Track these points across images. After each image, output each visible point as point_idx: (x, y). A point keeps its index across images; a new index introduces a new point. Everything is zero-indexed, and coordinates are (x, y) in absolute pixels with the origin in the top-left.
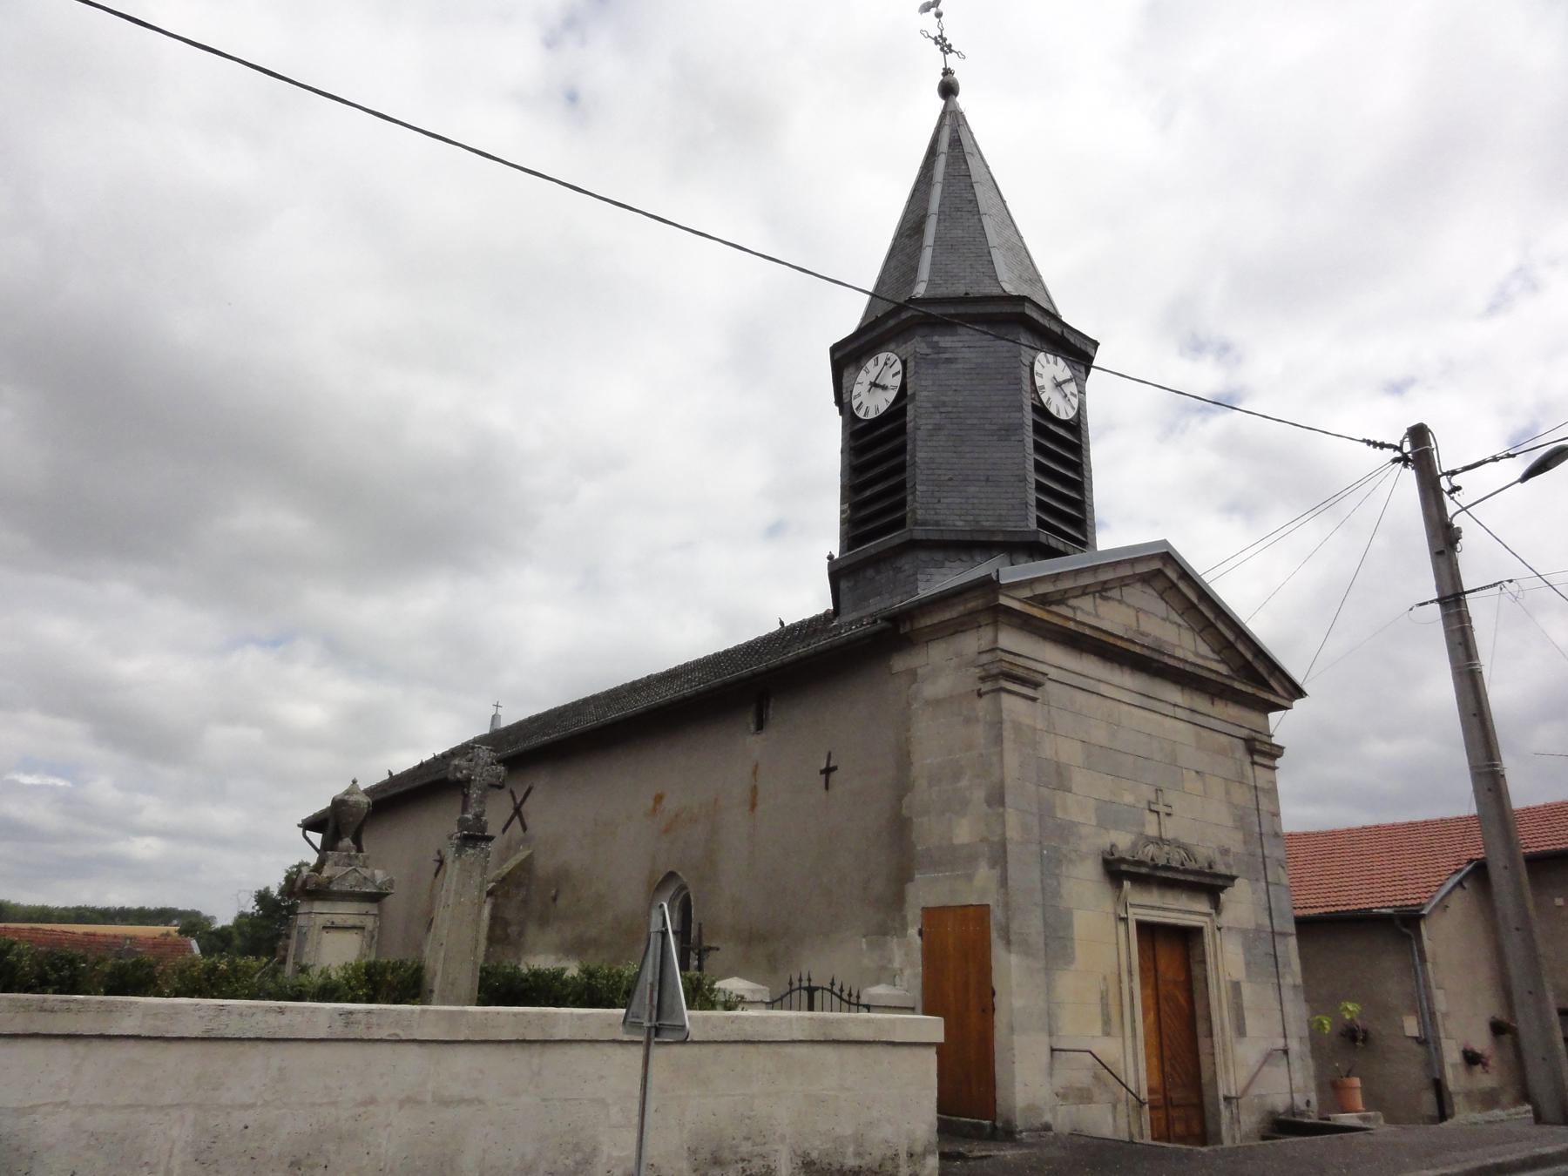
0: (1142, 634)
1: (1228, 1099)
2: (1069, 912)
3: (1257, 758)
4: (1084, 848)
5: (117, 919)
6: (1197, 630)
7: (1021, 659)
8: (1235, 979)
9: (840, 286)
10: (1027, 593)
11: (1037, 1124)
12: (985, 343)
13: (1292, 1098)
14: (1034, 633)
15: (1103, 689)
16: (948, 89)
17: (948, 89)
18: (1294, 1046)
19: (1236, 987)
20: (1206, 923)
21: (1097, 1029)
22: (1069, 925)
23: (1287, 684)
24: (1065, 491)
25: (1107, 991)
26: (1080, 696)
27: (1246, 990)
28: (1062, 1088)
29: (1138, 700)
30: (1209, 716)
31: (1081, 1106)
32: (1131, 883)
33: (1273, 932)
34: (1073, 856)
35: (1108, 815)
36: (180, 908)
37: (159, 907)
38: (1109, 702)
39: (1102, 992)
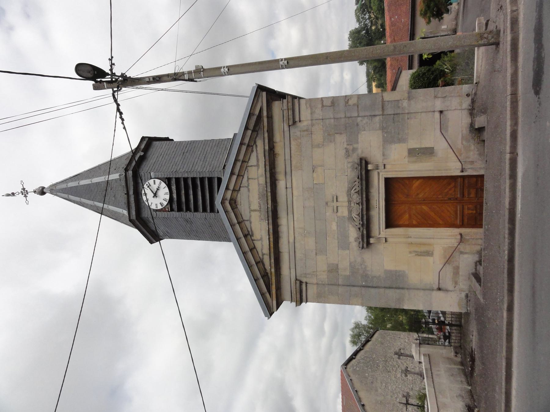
0: (260, 207)
1: (462, 171)
2: (386, 271)
3: (297, 119)
4: (359, 260)
5: (370, 88)
6: (246, 163)
7: (292, 290)
8: (406, 153)
9: (195, 368)
10: (268, 295)
11: (465, 301)
12: (158, 228)
13: (464, 109)
14: (280, 281)
15: (291, 240)
16: (42, 192)
17: (42, 192)
18: (439, 105)
19: (412, 152)
20: (382, 175)
21: (430, 259)
22: (391, 271)
23: (255, 102)
24: (199, 188)
25: (416, 252)
26: (298, 255)
27: (413, 144)
28: (452, 285)
29: (290, 216)
30: (285, 160)
31: (460, 274)
32: (370, 238)
33: (383, 115)
34: (363, 266)
35: (344, 245)
36: (366, 70)
37: (366, 77)
38: (296, 236)
39: (416, 255)
